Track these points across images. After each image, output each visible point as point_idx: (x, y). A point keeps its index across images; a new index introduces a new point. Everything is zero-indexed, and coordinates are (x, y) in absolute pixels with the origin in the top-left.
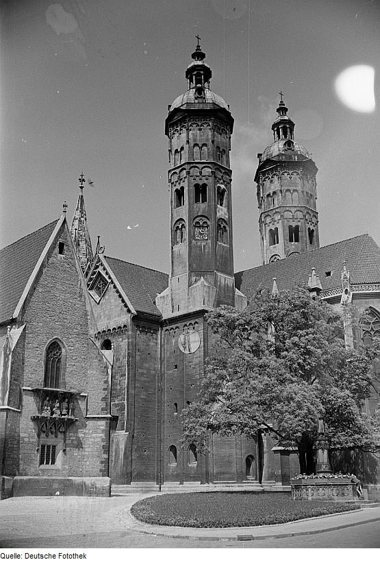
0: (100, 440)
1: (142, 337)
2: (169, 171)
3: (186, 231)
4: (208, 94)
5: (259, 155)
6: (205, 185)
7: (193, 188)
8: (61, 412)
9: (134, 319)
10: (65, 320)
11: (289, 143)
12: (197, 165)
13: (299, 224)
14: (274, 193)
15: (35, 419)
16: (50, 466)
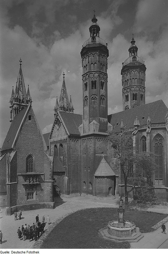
0: (49, 189)
1: (72, 143)
2: (82, 76)
3: (88, 101)
4: (97, 39)
5: (123, 63)
6: (95, 81)
7: (91, 83)
8: (33, 181)
9: (69, 137)
10: (33, 147)
11: (134, 57)
12: (92, 73)
13: (137, 93)
14: (128, 80)
15: (23, 185)
16: (31, 200)
